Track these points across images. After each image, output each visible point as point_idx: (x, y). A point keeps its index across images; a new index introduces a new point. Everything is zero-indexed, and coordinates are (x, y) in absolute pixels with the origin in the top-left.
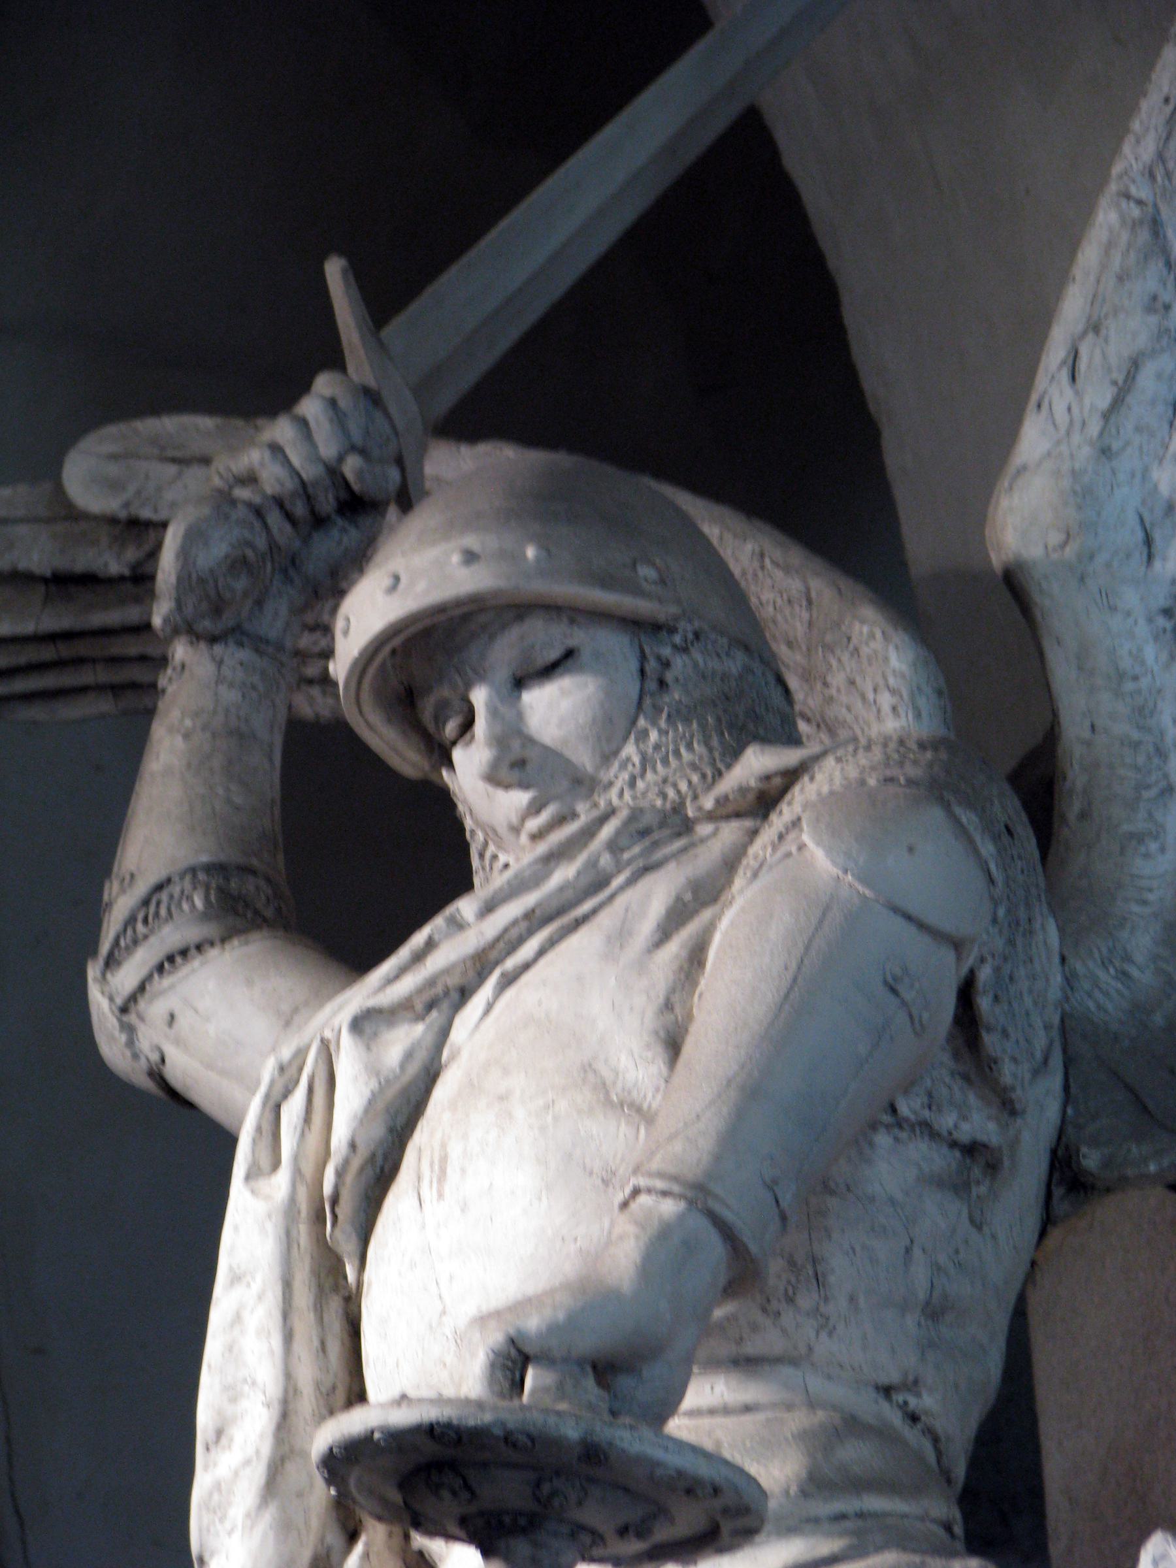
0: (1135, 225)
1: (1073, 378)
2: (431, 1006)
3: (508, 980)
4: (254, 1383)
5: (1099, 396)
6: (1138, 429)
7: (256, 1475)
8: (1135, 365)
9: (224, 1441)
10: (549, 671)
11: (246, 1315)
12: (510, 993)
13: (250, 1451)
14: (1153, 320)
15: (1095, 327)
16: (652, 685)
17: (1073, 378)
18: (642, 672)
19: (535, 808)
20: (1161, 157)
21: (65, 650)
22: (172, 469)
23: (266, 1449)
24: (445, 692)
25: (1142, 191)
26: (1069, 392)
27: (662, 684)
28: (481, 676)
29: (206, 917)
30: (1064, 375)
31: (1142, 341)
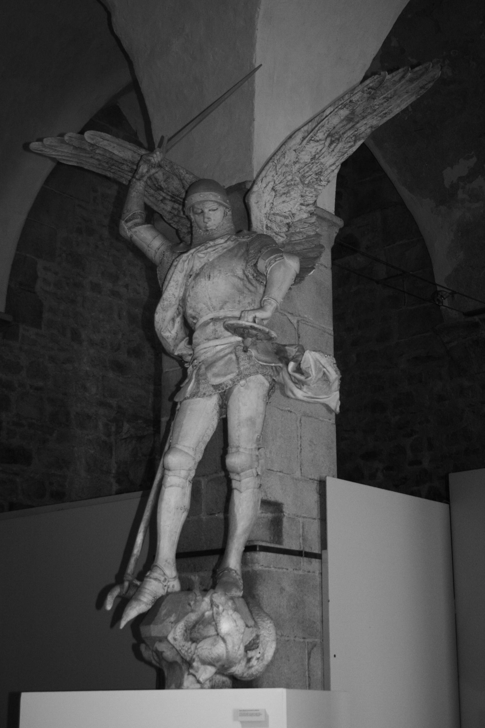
0: (274, 166)
1: (262, 182)
5: (264, 185)
6: (268, 190)
8: (269, 183)
14: (272, 177)
15: (265, 176)
16: (225, 215)
17: (262, 182)
18: (224, 213)
20: (279, 159)
22: (102, 140)
25: (276, 162)
26: (261, 184)
27: (227, 215)
30: (260, 181)
31: (271, 180)
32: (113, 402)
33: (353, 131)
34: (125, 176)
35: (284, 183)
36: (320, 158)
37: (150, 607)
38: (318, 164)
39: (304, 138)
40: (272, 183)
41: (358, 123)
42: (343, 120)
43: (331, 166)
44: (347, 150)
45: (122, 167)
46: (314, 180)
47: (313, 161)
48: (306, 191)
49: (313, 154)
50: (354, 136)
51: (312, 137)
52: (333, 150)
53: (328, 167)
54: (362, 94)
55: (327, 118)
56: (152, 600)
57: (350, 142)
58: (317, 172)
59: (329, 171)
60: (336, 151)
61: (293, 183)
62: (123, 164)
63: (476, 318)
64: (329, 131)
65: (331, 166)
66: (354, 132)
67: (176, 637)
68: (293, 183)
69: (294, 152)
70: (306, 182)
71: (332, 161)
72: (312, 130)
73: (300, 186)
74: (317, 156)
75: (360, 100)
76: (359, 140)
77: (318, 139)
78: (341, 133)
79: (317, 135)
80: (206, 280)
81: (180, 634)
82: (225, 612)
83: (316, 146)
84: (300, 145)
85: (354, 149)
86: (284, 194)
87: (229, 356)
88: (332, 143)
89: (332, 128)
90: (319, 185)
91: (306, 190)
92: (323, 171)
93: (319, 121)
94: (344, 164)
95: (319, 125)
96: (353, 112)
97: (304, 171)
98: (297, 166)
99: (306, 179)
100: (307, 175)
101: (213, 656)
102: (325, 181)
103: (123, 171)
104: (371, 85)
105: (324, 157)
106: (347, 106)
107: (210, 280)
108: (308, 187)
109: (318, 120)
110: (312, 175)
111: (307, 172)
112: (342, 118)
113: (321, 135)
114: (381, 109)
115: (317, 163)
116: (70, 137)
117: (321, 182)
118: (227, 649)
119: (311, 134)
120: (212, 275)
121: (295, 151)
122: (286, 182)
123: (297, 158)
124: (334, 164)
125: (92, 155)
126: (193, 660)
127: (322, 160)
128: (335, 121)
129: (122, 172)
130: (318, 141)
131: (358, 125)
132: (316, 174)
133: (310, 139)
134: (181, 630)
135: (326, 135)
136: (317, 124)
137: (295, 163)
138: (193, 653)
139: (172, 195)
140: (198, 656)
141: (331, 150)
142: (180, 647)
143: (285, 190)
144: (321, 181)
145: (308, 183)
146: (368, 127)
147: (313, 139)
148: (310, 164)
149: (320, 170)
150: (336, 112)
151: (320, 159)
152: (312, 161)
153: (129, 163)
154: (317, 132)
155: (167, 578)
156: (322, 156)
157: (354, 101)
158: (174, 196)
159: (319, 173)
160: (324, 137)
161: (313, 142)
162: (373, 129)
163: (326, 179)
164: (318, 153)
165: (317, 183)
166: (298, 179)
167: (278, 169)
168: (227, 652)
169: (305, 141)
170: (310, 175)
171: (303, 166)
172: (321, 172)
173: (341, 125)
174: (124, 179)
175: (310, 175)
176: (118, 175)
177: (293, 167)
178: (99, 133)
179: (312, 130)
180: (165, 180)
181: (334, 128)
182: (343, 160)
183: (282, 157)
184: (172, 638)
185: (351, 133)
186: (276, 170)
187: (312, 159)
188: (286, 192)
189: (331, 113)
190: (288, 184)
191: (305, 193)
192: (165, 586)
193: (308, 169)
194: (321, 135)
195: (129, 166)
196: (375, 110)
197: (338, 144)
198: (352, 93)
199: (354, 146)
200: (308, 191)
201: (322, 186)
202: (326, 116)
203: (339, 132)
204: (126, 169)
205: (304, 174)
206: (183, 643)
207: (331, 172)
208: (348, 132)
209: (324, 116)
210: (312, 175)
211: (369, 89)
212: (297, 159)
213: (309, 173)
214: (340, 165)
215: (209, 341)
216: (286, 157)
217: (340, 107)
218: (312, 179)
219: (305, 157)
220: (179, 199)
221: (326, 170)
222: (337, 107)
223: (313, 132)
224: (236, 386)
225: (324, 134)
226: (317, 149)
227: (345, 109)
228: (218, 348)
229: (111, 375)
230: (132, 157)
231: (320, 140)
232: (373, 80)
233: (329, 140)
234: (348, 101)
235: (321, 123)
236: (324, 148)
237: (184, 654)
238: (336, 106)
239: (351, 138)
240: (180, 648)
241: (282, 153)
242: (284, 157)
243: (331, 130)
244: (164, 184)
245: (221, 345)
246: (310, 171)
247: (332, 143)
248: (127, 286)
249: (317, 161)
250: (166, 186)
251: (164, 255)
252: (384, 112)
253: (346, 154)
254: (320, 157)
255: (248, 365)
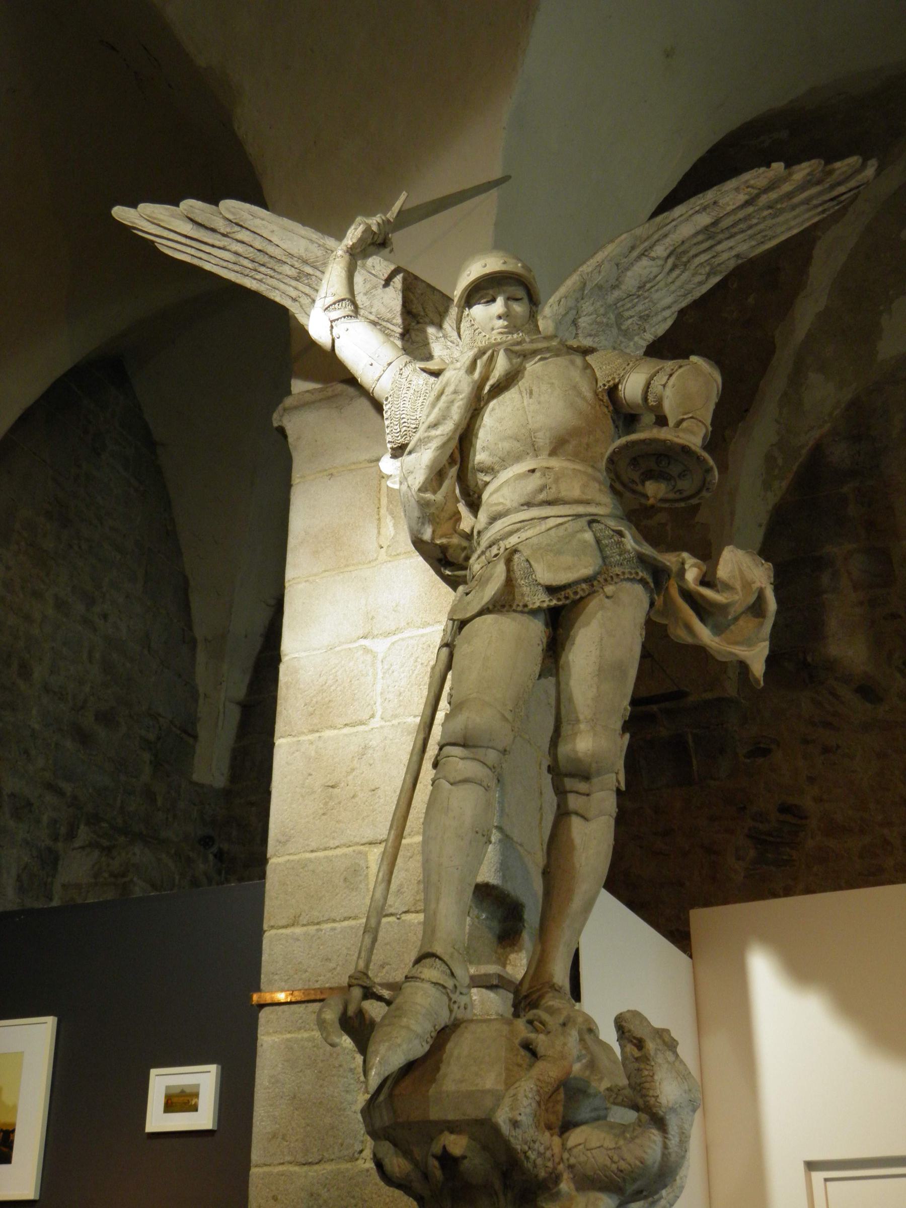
2: (519, 356)
3: (541, 359)
4: (452, 418)
7: (445, 438)
9: (435, 428)
10: (517, 300)
11: (455, 402)
12: (542, 362)
13: (445, 433)
19: (506, 327)
20: (592, 272)
21: (188, 242)
22: (251, 217)
23: (450, 435)
24: (491, 292)
28: (504, 292)
29: (352, 311)
30: (557, 304)
32: (67, 787)
33: (709, 256)
34: (282, 286)
35: (591, 317)
36: (653, 290)
37: (427, 1047)
38: (647, 300)
39: (633, 248)
40: (574, 312)
41: (719, 243)
42: (698, 233)
43: (664, 309)
44: (693, 288)
45: (281, 268)
46: (636, 327)
47: (640, 293)
48: (621, 342)
49: (644, 279)
50: (709, 264)
51: (646, 251)
52: (673, 282)
53: (659, 310)
54: (736, 194)
55: (674, 223)
56: (431, 1032)
57: (701, 274)
58: (642, 314)
59: (660, 317)
60: (678, 283)
61: (605, 320)
62: (285, 263)
63: (655, 708)
64: (674, 244)
65: (664, 309)
66: (711, 258)
67: (519, 1118)
68: (605, 320)
69: (616, 267)
70: (623, 327)
71: (668, 300)
72: (648, 238)
73: (615, 331)
74: (648, 286)
75: (731, 203)
76: (715, 274)
77: (653, 254)
78: (692, 253)
79: (655, 248)
80: (522, 397)
81: (528, 1110)
82: (660, 1055)
83: (652, 266)
84: (626, 258)
85: (704, 289)
86: (590, 335)
87: (579, 536)
88: (674, 267)
89: (680, 242)
90: (641, 338)
91: (621, 341)
92: (651, 315)
93: (661, 225)
94: (682, 312)
95: (660, 232)
96: (715, 224)
97: (623, 306)
98: (617, 294)
99: (624, 321)
100: (627, 314)
101: (623, 1165)
102: (651, 334)
103: (280, 277)
104: (752, 182)
105: (657, 291)
106: (708, 210)
107: (533, 397)
108: (625, 335)
109: (660, 224)
110: (634, 316)
111: (628, 310)
112: (699, 228)
113: (660, 251)
114: (761, 227)
115: (645, 298)
116: (191, 206)
117: (645, 334)
118: (665, 1147)
119: (646, 244)
120: (535, 389)
121: (617, 265)
122: (595, 316)
123: (617, 280)
124: (669, 307)
125: (226, 243)
126: (556, 1178)
127: (656, 296)
128: (686, 230)
129: (278, 280)
130: (653, 259)
131: (719, 248)
132: (640, 317)
133: (642, 252)
134: (530, 1101)
135: (668, 251)
136: (656, 229)
137: (614, 287)
138: (557, 1160)
139: (377, 319)
140: (571, 1167)
141: (670, 280)
142: (526, 1143)
143: (592, 330)
144: (645, 331)
145: (626, 331)
146: (734, 253)
147: (646, 253)
148: (635, 297)
149: (647, 312)
150: (690, 216)
151: (651, 292)
152: (638, 291)
153: (297, 261)
154: (655, 242)
155: (458, 984)
156: (656, 288)
157: (720, 204)
158: (380, 322)
159: (645, 317)
160: (665, 254)
161: (646, 258)
162: (740, 261)
163: (653, 329)
164: (649, 281)
165: (639, 334)
166: (612, 317)
167: (586, 292)
168: (665, 1155)
169: (635, 254)
170: (631, 317)
171: (624, 297)
172: (648, 316)
173: (695, 240)
174: (277, 291)
175: (631, 317)
176: (268, 285)
177: (609, 293)
178: (247, 206)
179: (648, 238)
180: (367, 292)
181: (683, 242)
182: (683, 304)
183: (595, 271)
184: (508, 1121)
185: (706, 258)
186: (583, 291)
187: (640, 288)
188: (593, 333)
189: (681, 215)
190: (598, 320)
191: (620, 345)
192: (455, 1002)
193: (630, 305)
194: (660, 251)
195: (296, 268)
196: (750, 227)
197: (683, 272)
198: (719, 191)
199: (704, 284)
200: (624, 344)
201: (645, 340)
202: (673, 220)
203: (688, 252)
204: (289, 273)
205: (623, 312)
206: (531, 1133)
207: (662, 321)
208: (702, 256)
209: (671, 218)
210: (634, 316)
211: (748, 187)
212: (617, 283)
213: (631, 313)
214: (676, 313)
215: (531, 508)
216: (603, 274)
217: (697, 208)
218: (632, 324)
219: (630, 281)
220: (389, 325)
221: (656, 314)
222: (692, 209)
223: (650, 241)
224: (595, 594)
225: (666, 249)
226: (651, 272)
227: (704, 213)
228: (552, 522)
229: (69, 744)
230: (306, 250)
231: (658, 258)
232: (755, 174)
233: (671, 261)
234: (713, 201)
235: (665, 228)
236: (660, 273)
237: (534, 1161)
238: (691, 206)
239: (705, 267)
240: (526, 1148)
241: (597, 264)
242: (600, 272)
243: (677, 244)
244: (365, 298)
245: (558, 516)
246: (633, 310)
247: (674, 267)
248: (105, 617)
249: (646, 294)
250: (367, 304)
251: (401, 374)
252: (763, 234)
253: (690, 295)
254: (652, 287)
255: (618, 557)
